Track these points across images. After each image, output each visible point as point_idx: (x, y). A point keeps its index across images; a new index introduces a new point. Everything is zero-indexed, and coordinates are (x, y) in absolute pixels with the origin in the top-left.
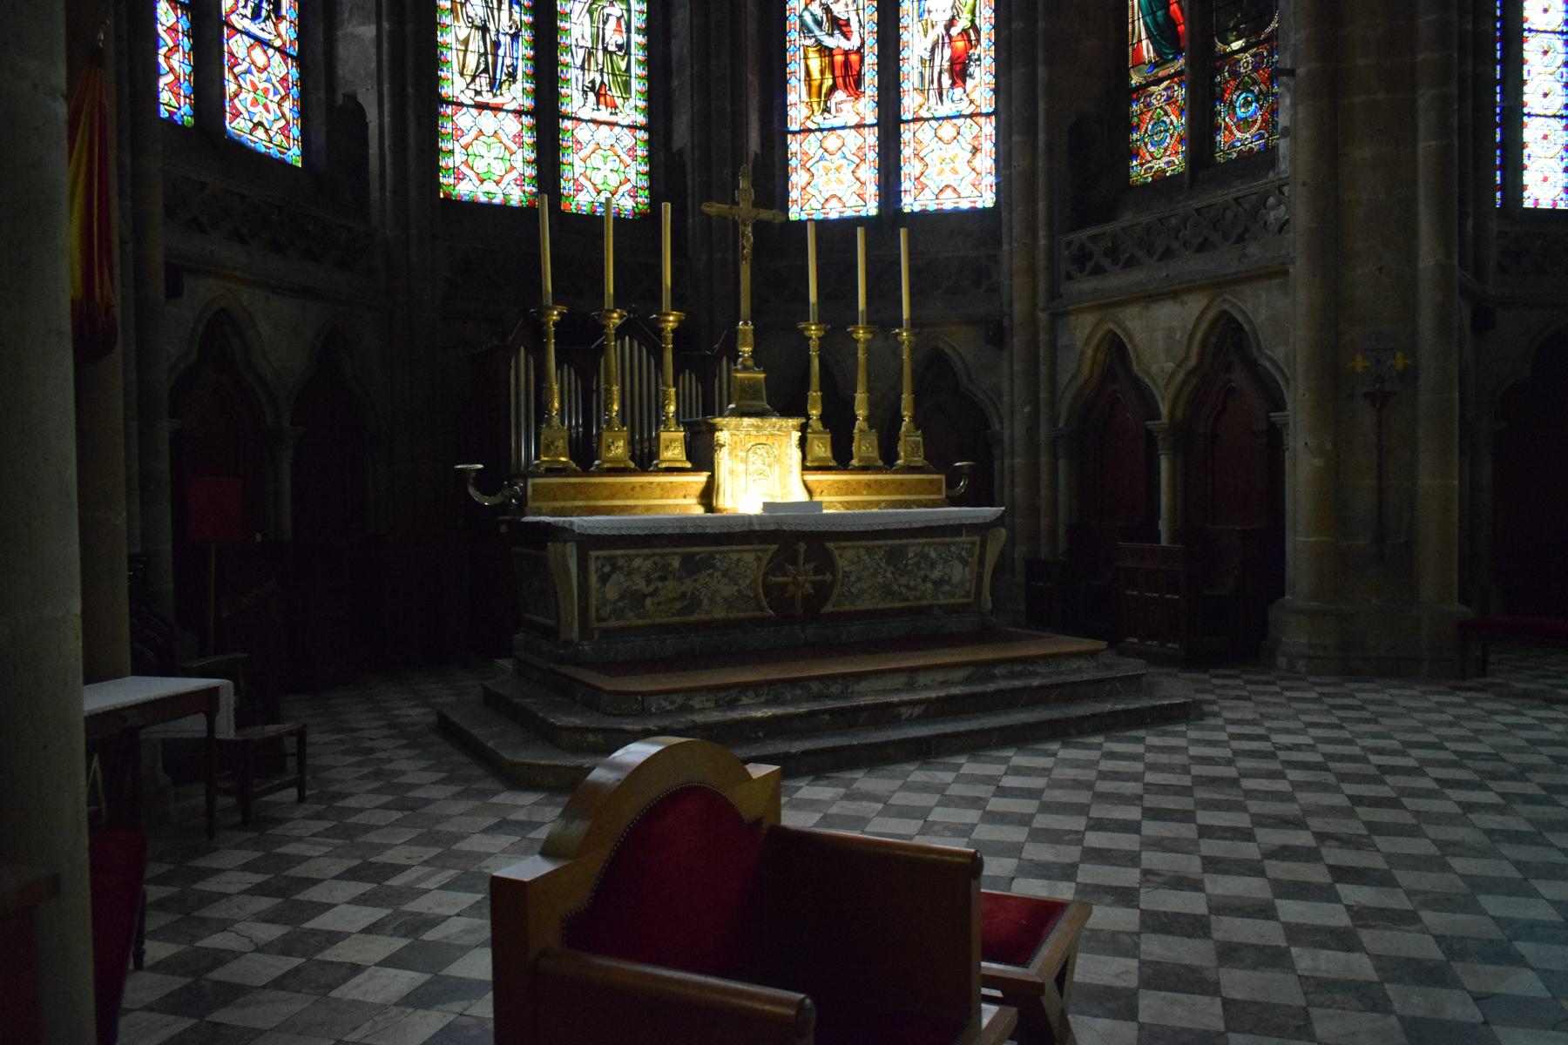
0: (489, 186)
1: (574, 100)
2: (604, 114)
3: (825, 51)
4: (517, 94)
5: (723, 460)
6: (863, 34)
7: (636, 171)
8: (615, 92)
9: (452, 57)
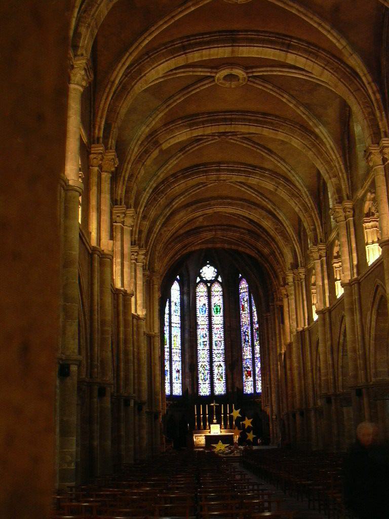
0: (205, 393)
1: (216, 381)
2: (220, 382)
3: (247, 371)
4: (208, 382)
7: (224, 389)
8: (221, 379)
9: (200, 378)
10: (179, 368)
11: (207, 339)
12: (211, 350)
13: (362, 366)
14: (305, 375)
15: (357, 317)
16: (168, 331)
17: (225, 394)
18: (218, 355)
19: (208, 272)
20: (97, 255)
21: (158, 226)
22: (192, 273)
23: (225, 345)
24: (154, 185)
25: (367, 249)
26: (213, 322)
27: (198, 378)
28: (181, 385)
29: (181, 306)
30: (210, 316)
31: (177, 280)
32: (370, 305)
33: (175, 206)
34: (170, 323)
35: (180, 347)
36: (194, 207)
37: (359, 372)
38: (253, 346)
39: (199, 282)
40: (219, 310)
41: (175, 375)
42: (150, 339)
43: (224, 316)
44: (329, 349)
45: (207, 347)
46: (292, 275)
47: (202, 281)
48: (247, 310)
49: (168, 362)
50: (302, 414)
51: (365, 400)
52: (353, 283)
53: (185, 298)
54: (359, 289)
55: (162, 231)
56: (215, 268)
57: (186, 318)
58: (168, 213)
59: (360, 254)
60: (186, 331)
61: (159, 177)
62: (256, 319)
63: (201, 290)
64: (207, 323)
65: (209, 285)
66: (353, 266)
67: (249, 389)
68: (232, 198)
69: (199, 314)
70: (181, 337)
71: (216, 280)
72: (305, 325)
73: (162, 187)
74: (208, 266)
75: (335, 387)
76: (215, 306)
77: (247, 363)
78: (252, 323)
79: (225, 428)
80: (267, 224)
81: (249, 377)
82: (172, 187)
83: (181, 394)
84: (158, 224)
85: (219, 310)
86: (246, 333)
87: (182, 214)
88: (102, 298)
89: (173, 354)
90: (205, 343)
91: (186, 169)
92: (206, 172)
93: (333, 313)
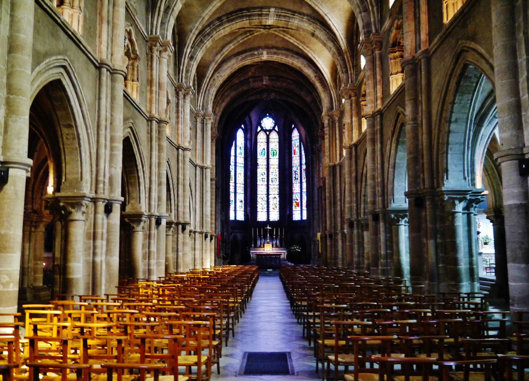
2: (274, 210)
3: (296, 202)
4: (265, 210)
5: (265, 247)
6: (299, 201)
8: (275, 208)
10: (243, 199)
11: (265, 176)
12: (268, 185)
13: (380, 192)
14: (335, 203)
15: (378, 146)
16: (234, 169)
17: (278, 221)
18: (274, 190)
19: (268, 123)
20: (105, 70)
21: (211, 71)
22: (254, 123)
23: (279, 181)
24: (200, 27)
25: (391, 79)
26: (270, 163)
27: (256, 207)
28: (243, 212)
29: (244, 150)
30: (268, 159)
31: (242, 128)
32: (390, 134)
33: (226, 53)
34: (236, 163)
35: (243, 182)
36: (244, 55)
37: (377, 199)
38: (301, 183)
39: (260, 131)
40: (275, 154)
41: (239, 204)
42: (203, 169)
43: (279, 159)
44: (353, 181)
45: (266, 183)
46: (328, 117)
47: (262, 129)
48: (298, 154)
49: (233, 194)
50: (331, 236)
51: (382, 224)
52: (376, 114)
53: (248, 144)
54: (381, 120)
55: (215, 77)
56: (273, 119)
57: (249, 159)
58: (219, 59)
59: (384, 86)
60: (249, 170)
61: (203, 18)
62: (304, 161)
63: (262, 137)
64: (265, 163)
65: (268, 133)
66: (377, 97)
67: (296, 217)
68: (277, 48)
69: (259, 156)
70: (244, 175)
71: (274, 129)
72: (336, 161)
73: (208, 30)
74: (268, 118)
75: (358, 214)
76: (272, 151)
77: (297, 196)
78: (301, 164)
79: (277, 247)
80: (309, 72)
81: (297, 207)
82: (217, 30)
83: (243, 220)
84: (210, 69)
85: (275, 154)
86: (296, 172)
87: (233, 61)
88: (113, 114)
89: (237, 188)
90: (264, 180)
91: (231, 13)
92: (249, 16)
93: (359, 147)
